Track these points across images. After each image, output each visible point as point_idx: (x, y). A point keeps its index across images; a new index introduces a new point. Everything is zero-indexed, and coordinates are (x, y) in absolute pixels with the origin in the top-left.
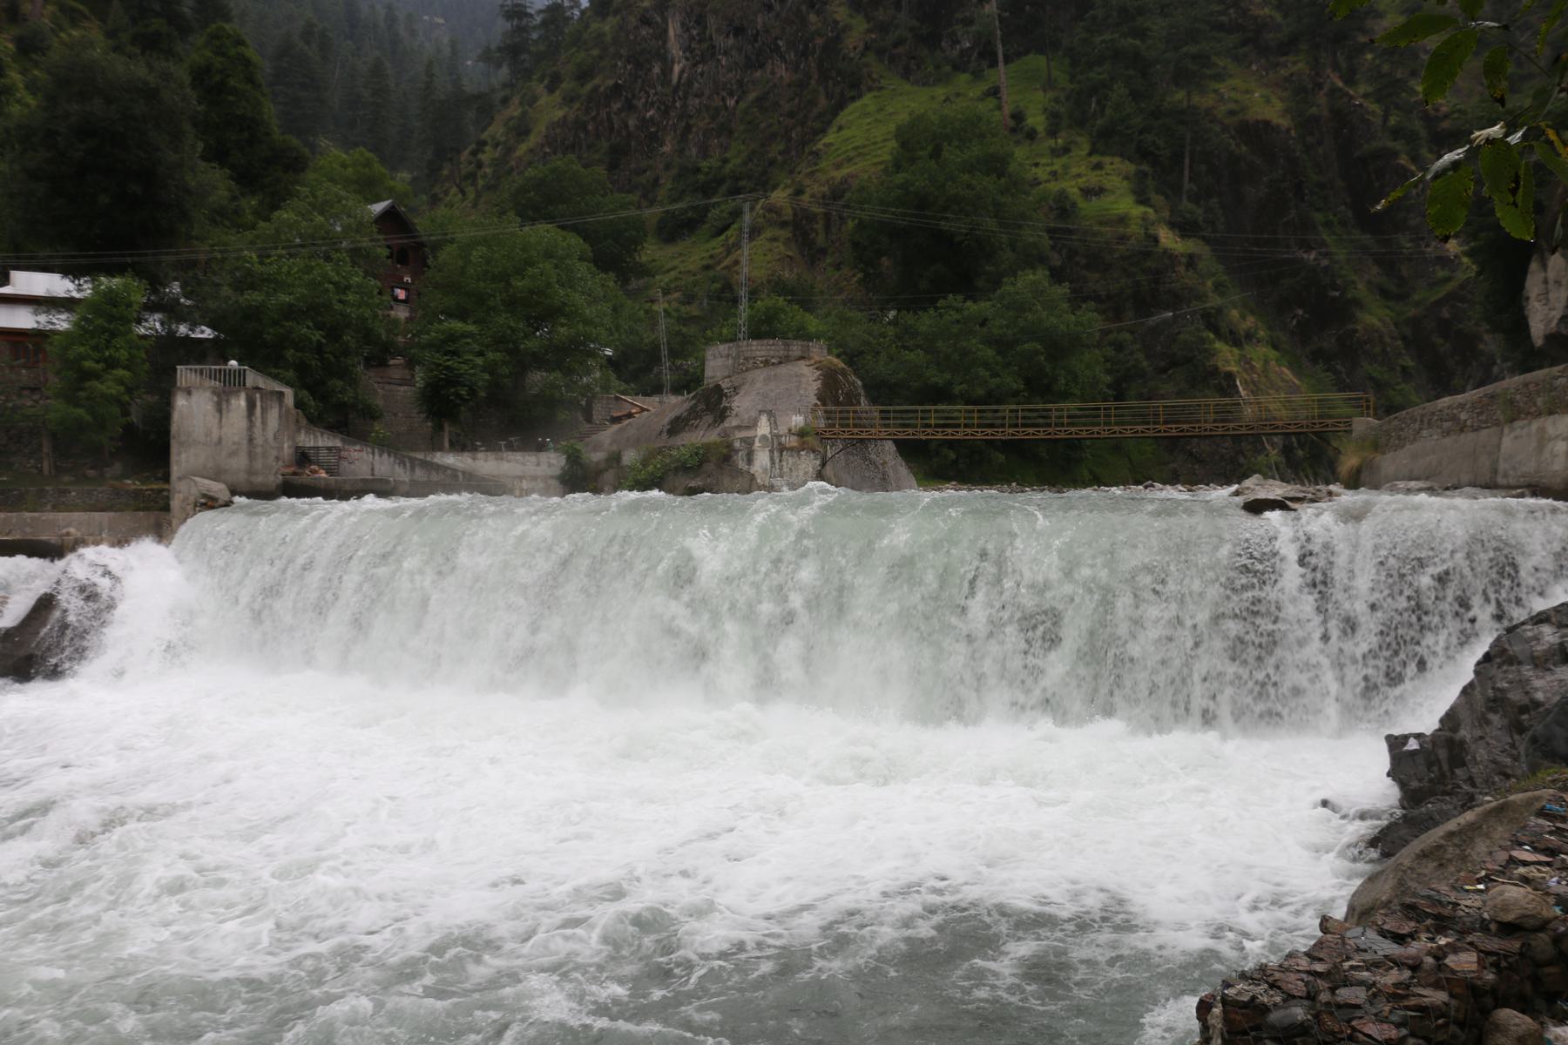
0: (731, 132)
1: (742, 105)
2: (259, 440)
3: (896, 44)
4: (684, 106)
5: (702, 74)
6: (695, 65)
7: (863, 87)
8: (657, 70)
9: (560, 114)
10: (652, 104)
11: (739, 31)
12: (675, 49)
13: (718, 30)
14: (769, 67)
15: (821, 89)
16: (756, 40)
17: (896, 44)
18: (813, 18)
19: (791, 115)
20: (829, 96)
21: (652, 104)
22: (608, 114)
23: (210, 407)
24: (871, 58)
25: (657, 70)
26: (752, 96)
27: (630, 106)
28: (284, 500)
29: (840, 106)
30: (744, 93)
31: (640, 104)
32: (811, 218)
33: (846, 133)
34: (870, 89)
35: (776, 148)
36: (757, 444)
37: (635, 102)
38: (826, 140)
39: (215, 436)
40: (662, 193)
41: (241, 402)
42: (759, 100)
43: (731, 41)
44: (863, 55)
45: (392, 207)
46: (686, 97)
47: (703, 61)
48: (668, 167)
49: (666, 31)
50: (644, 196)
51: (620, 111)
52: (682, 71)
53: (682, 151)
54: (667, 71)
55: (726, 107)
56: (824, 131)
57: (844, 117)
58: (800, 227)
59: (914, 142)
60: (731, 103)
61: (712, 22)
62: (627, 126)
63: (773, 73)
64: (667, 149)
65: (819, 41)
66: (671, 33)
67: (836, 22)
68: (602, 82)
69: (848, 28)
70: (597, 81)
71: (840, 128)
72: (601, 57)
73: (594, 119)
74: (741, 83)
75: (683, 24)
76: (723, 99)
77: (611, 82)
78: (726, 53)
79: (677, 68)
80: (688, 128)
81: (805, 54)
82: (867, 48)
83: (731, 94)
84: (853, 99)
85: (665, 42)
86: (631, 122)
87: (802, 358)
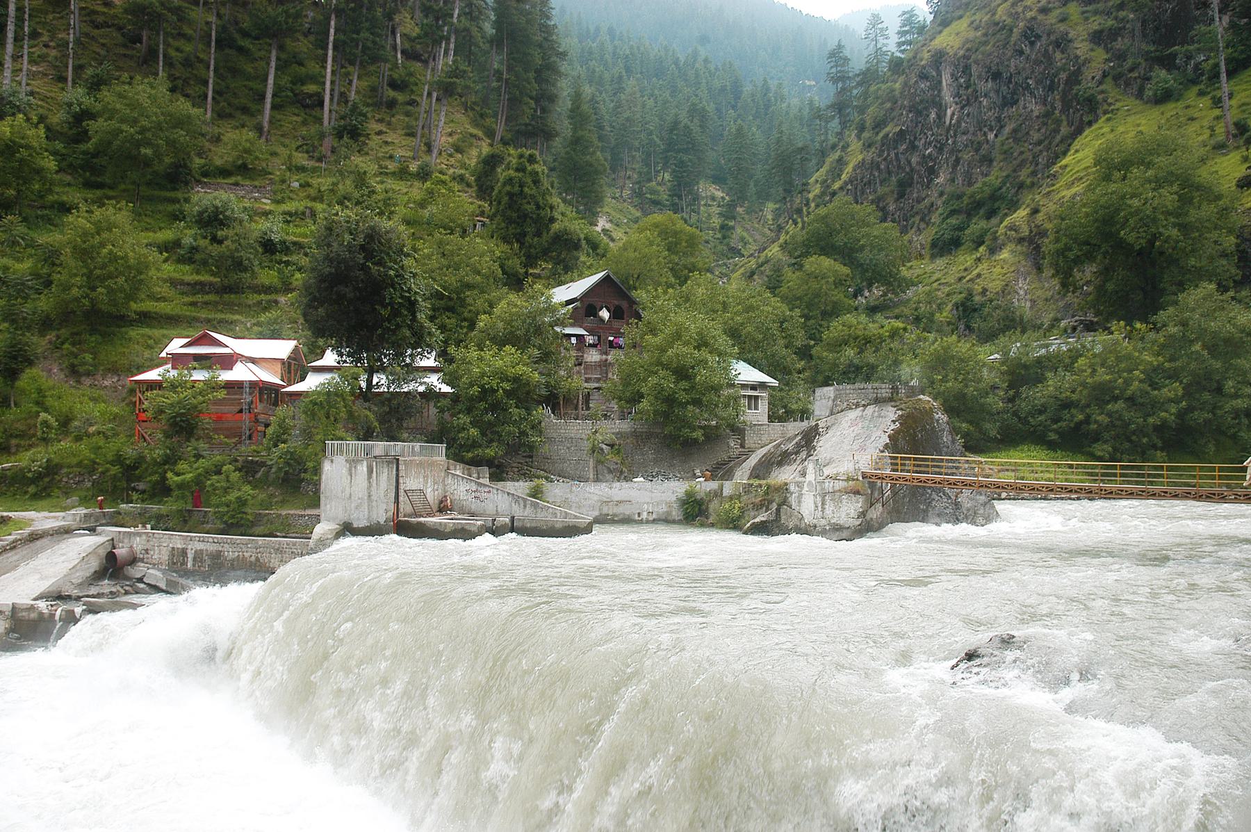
0: (991, 161)
1: (1000, 138)
2: (374, 498)
3: (1131, 70)
4: (954, 143)
5: (968, 115)
6: (962, 108)
7: (1100, 112)
8: (933, 115)
9: (860, 157)
10: (930, 144)
11: (996, 76)
12: (947, 96)
13: (980, 77)
14: (1021, 103)
15: (1064, 117)
16: (1010, 82)
17: (1131, 70)
18: (1058, 55)
19: (1040, 143)
20: (1070, 124)
21: (930, 144)
22: (896, 155)
23: (345, 471)
24: (1108, 85)
25: (933, 115)
26: (1007, 130)
27: (913, 147)
28: (395, 537)
29: (1079, 131)
30: (1002, 127)
31: (920, 144)
32: (1043, 234)
33: (1079, 155)
34: (1105, 113)
35: (1023, 174)
36: (806, 488)
37: (917, 143)
38: (1064, 162)
39: (347, 493)
40: (935, 218)
41: (363, 468)
42: (1015, 131)
43: (990, 84)
44: (1100, 83)
45: (607, 279)
46: (955, 135)
47: (968, 103)
48: (941, 194)
49: (940, 82)
50: (922, 220)
51: (906, 150)
52: (953, 114)
53: (953, 180)
54: (941, 117)
55: (988, 141)
56: (1065, 153)
57: (1077, 144)
58: (1032, 242)
59: (1112, 166)
60: (991, 136)
61: (975, 70)
62: (909, 162)
63: (1025, 108)
64: (940, 180)
65: (1063, 76)
66: (944, 83)
67: (1077, 57)
68: (891, 129)
69: (1087, 61)
70: (887, 129)
71: (1077, 151)
72: (892, 109)
73: (885, 159)
74: (999, 119)
75: (952, 75)
76: (985, 134)
77: (898, 129)
78: (986, 96)
79: (949, 112)
80: (957, 161)
81: (1051, 88)
82: (1105, 75)
83: (991, 130)
84: (1090, 124)
85: (940, 91)
86: (914, 160)
87: (891, 399)
